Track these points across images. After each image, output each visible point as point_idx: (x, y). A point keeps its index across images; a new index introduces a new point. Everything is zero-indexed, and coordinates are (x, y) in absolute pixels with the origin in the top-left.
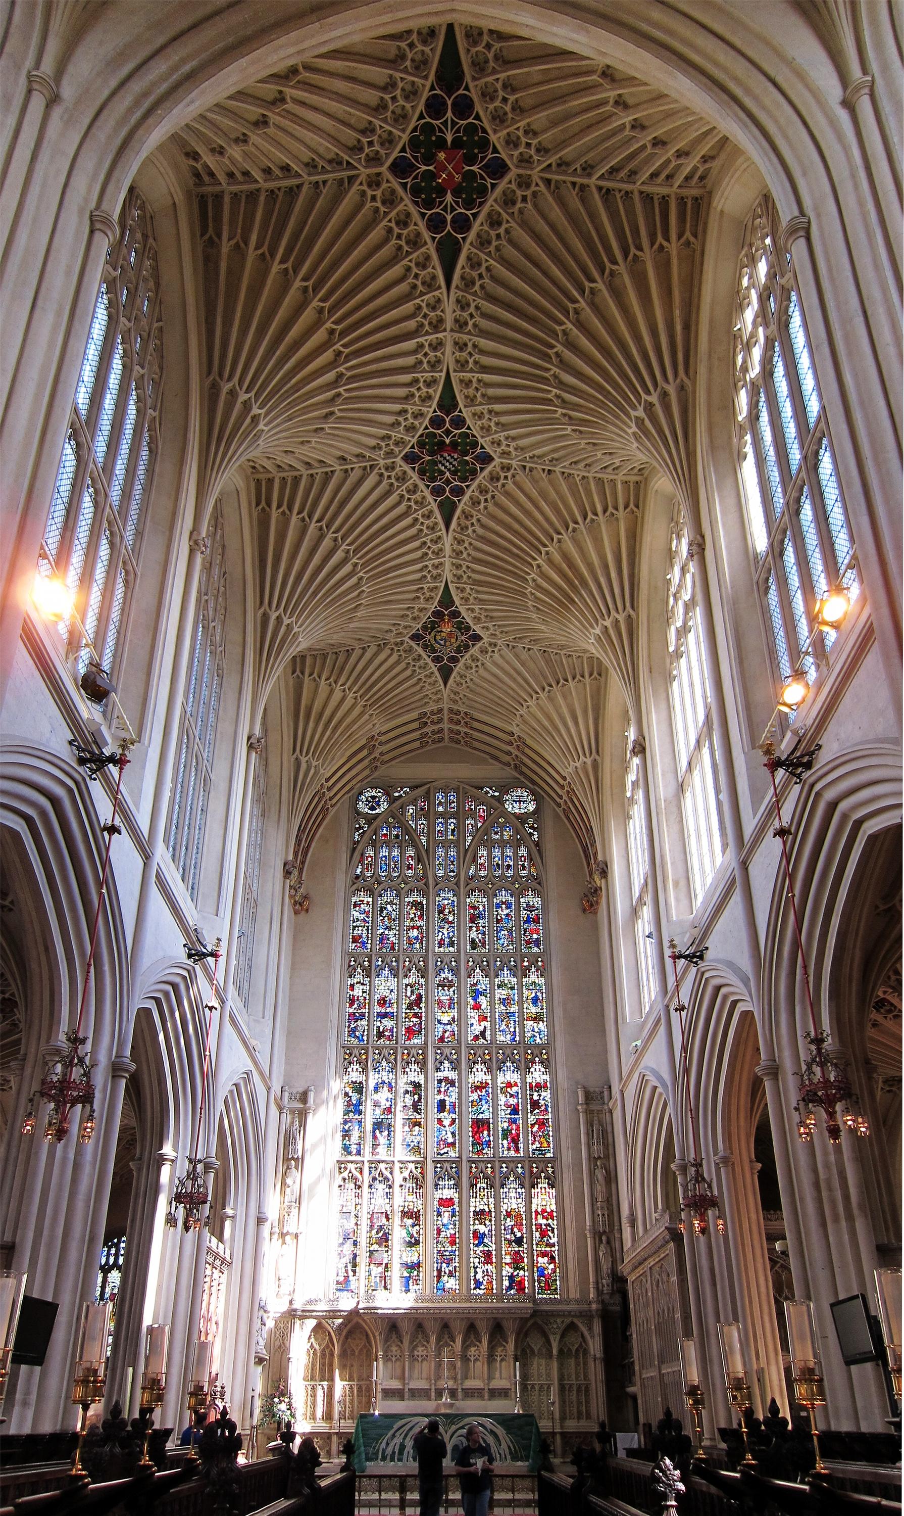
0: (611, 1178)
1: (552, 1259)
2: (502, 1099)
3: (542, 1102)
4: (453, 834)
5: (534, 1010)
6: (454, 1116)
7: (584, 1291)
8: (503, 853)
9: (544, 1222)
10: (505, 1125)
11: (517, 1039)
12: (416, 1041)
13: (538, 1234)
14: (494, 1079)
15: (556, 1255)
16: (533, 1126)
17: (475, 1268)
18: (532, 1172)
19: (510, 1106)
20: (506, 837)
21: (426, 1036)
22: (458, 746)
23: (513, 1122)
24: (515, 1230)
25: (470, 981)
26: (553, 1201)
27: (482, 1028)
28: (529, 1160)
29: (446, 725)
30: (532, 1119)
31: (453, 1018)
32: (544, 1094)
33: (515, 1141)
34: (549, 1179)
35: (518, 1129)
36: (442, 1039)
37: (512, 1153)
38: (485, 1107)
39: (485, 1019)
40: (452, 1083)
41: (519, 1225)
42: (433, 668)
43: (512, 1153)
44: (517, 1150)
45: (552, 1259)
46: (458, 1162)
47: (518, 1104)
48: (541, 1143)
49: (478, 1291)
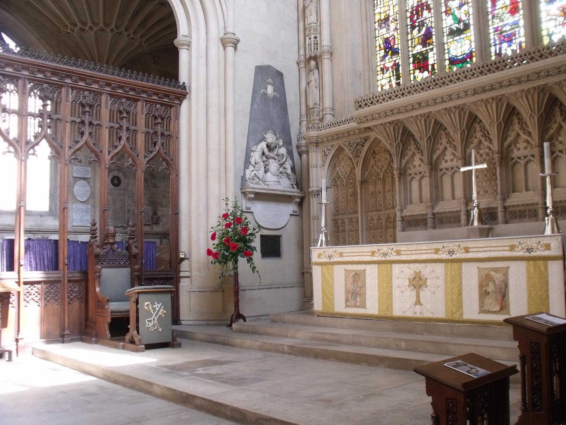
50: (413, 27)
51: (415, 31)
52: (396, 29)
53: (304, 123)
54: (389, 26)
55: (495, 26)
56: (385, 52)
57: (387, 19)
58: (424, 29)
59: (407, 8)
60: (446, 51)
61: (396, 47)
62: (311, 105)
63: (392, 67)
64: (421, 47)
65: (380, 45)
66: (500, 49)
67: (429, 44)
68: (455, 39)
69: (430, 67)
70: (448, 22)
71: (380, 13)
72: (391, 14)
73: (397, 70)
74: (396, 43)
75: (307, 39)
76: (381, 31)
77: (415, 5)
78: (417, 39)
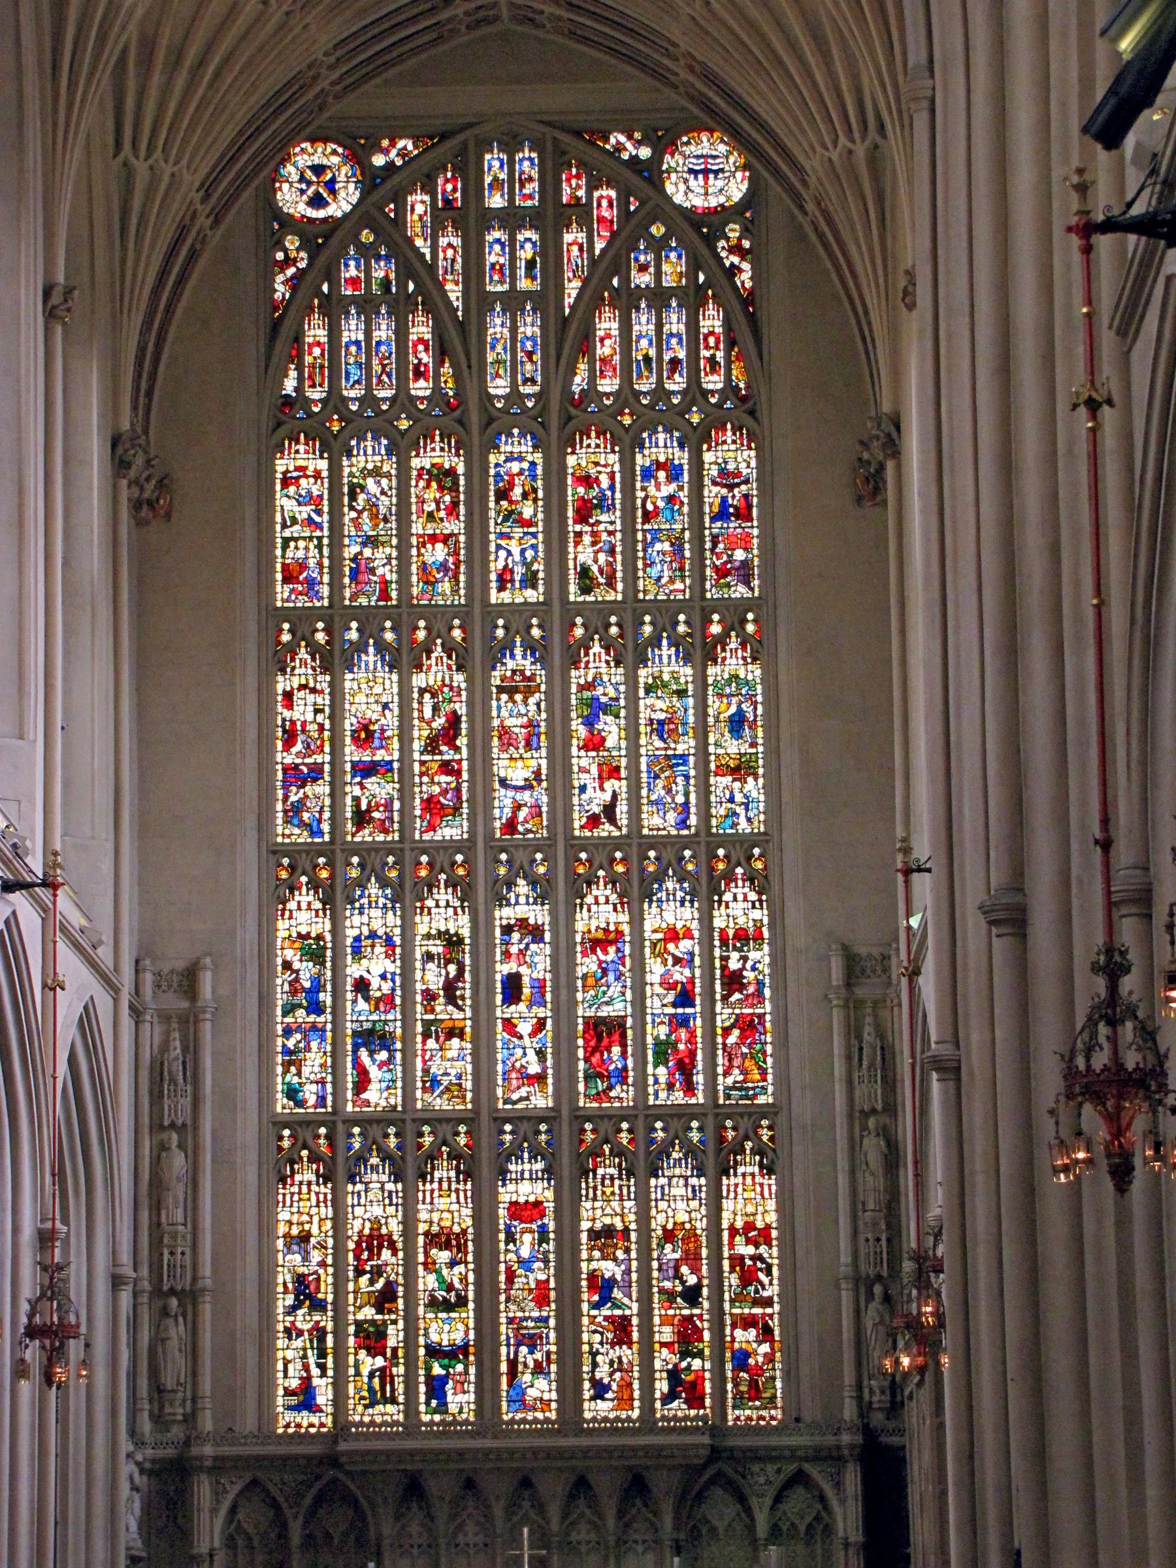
2: (655, 970)
3: (749, 975)
4: (530, 275)
6: (541, 1012)
8: (659, 326)
9: (750, 1250)
11: (693, 820)
12: (451, 831)
13: (734, 1280)
14: (637, 921)
15: (775, 1323)
16: (727, 1032)
17: (594, 1354)
18: (722, 1139)
19: (673, 986)
20: (668, 282)
21: (472, 818)
22: (541, 34)
23: (681, 1022)
24: (684, 1269)
25: (577, 677)
26: (771, 1205)
27: (607, 797)
28: (714, 1113)
30: (724, 1015)
31: (537, 773)
32: (753, 955)
33: (685, 1068)
34: (762, 1154)
35: (692, 1038)
36: (511, 826)
37: (678, 1097)
38: (615, 990)
39: (614, 772)
40: (536, 933)
41: (694, 1259)
44: (689, 1089)
45: (766, 1334)
46: (549, 1117)
47: (691, 981)
48: (745, 1072)
50: (359, 1272)
51: (364, 1280)
52: (323, 1264)
53: (146, 1414)
54: (308, 1253)
55: (511, 1315)
56: (297, 1298)
57: (305, 1237)
58: (382, 1281)
59: (350, 1233)
60: (422, 1332)
61: (320, 1296)
62: (169, 1383)
63: (310, 1332)
64: (373, 1311)
65: (285, 1284)
66: (516, 1353)
67: (390, 1312)
68: (440, 1315)
69: (389, 1351)
71: (290, 1223)
72: (315, 1231)
73: (322, 1338)
74: (323, 1289)
75: (166, 1252)
76: (289, 1257)
77: (367, 1232)
78: (366, 1296)
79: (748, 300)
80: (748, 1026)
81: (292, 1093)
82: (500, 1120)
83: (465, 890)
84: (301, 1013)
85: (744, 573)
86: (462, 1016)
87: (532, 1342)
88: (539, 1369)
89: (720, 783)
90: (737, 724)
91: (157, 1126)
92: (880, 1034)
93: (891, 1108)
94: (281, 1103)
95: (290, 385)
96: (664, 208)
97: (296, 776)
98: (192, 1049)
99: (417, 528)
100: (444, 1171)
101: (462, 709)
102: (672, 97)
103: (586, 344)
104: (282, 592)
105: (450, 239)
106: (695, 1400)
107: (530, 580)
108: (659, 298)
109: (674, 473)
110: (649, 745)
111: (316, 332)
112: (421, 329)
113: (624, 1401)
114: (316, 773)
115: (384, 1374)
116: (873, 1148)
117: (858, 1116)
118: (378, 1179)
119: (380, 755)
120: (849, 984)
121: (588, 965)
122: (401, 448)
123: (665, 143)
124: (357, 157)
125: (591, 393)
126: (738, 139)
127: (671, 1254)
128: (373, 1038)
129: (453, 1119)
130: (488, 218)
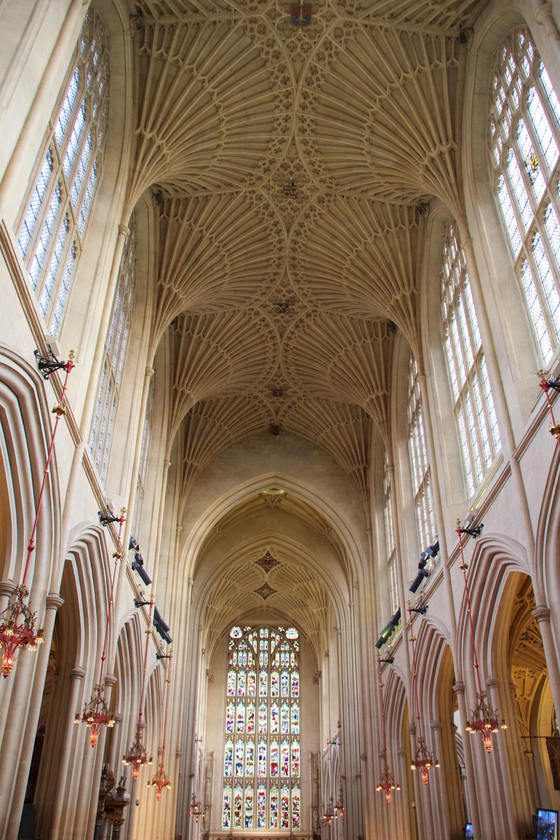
0: (318, 787)
1: (298, 815)
2: (282, 755)
5: (294, 720)
6: (265, 762)
7: (308, 828)
10: (283, 765)
12: (252, 732)
13: (293, 806)
23: (286, 764)
25: (272, 708)
28: (291, 778)
29: (264, 608)
30: (293, 763)
33: (286, 771)
37: (285, 776)
40: (264, 749)
41: (287, 803)
42: (261, 597)
43: (285, 776)
45: (298, 815)
46: (266, 778)
49: (273, 827)
70: (246, 806)
79: (298, 652)
80: (296, 765)
81: (226, 773)
82: (258, 779)
83: (254, 741)
84: (228, 761)
85: (297, 693)
86: (253, 762)
87: (262, 816)
88: (263, 821)
89: (293, 726)
90: (295, 717)
91: (206, 778)
92: (317, 766)
93: (318, 779)
94: (225, 775)
95: (231, 663)
96: (285, 638)
97: (229, 722)
98: (212, 766)
99: (249, 684)
100: (249, 787)
101: (254, 713)
102: (287, 623)
103: (274, 658)
104: (229, 694)
105: (255, 642)
106: (287, 826)
107: (265, 693)
108: (285, 652)
109: (287, 678)
110: (282, 720)
111: (235, 654)
112: (250, 655)
113: (276, 826)
114: (232, 722)
115: (239, 821)
116: (315, 785)
117: (313, 780)
118: (239, 788)
119: (242, 720)
120: (312, 759)
121: (272, 754)
122: (247, 672)
123: (286, 629)
124: (242, 629)
125: (275, 666)
126: (297, 629)
127: (284, 802)
128: (239, 765)
129: (251, 779)
130: (261, 639)
